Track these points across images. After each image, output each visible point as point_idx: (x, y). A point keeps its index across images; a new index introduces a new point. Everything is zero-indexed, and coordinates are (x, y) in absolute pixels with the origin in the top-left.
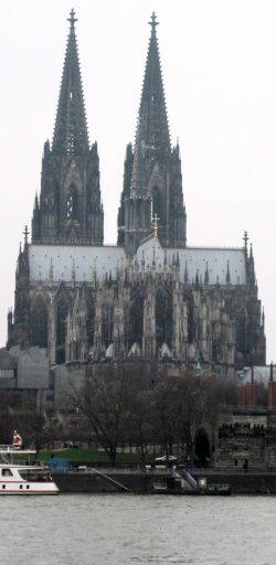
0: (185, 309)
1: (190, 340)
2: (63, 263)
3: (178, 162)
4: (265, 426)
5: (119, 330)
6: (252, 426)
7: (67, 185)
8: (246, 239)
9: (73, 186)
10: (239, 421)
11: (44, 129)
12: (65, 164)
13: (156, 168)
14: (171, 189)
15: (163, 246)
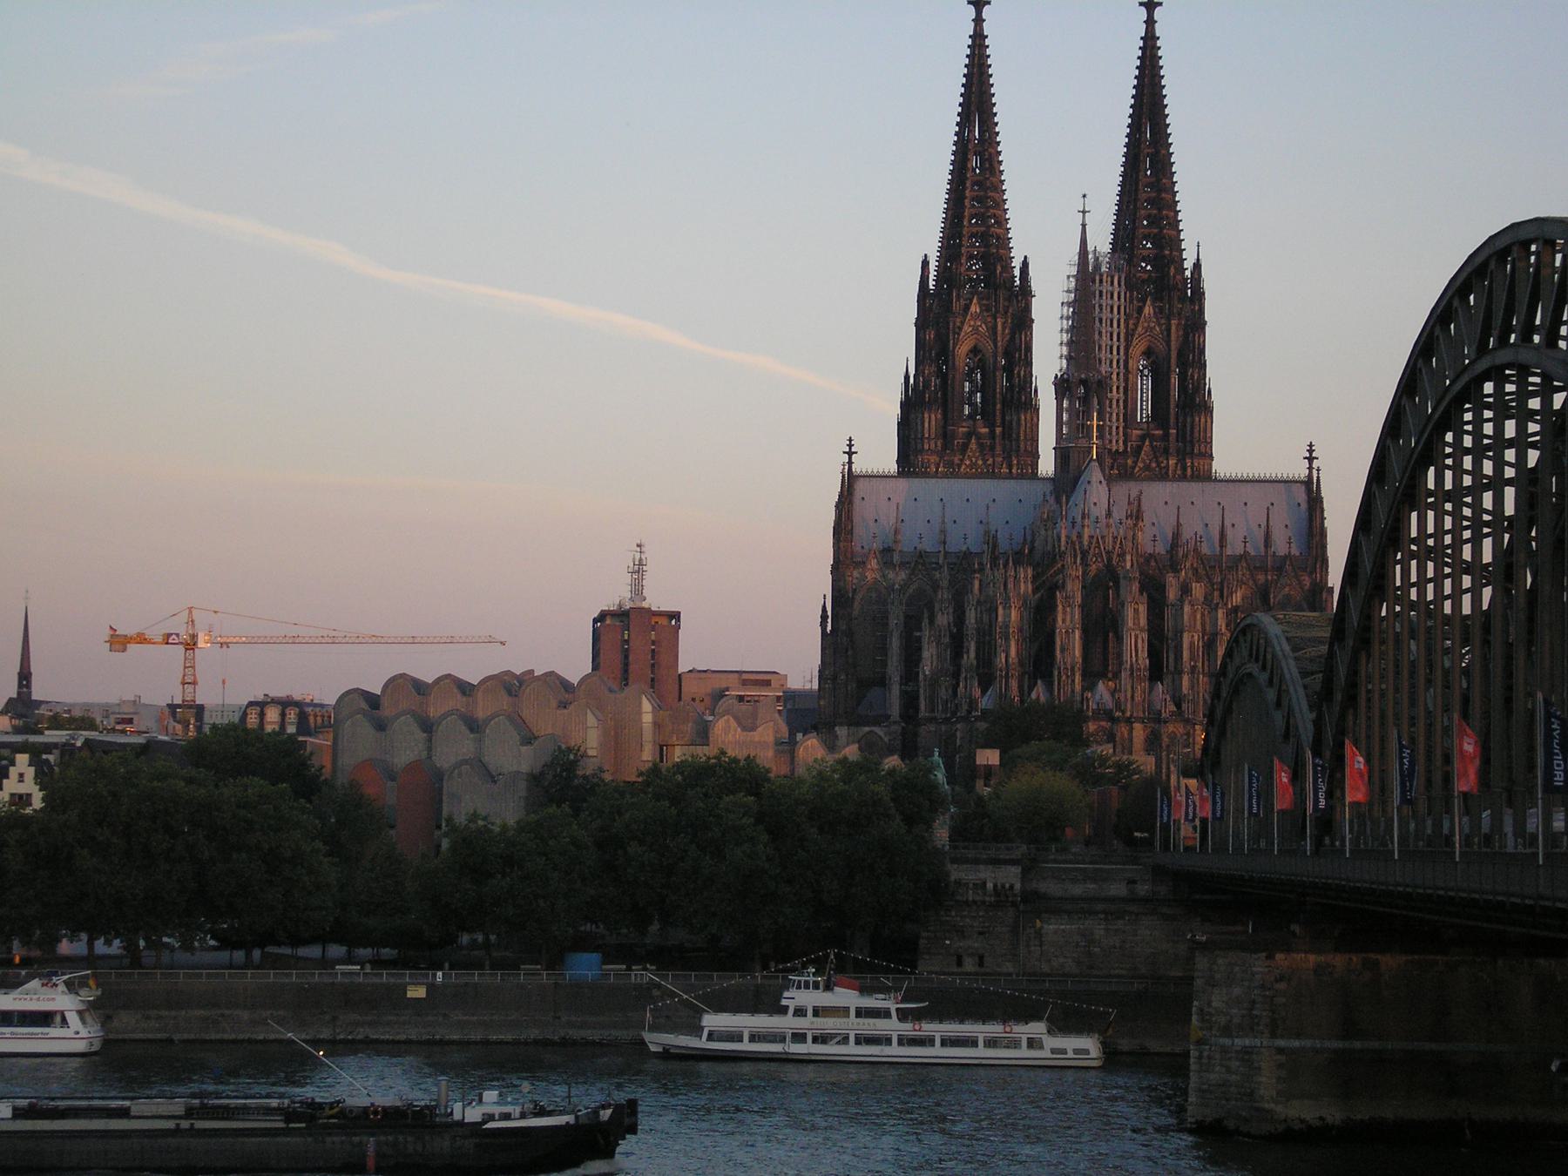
0: (1143, 609)
1: (1156, 672)
2: (969, 505)
3: (1199, 295)
4: (1018, 886)
5: (1010, 653)
6: (990, 885)
7: (962, 350)
8: (1311, 459)
9: (975, 351)
10: (963, 875)
11: (921, 232)
12: (957, 306)
13: (1148, 310)
14: (1180, 354)
15: (1110, 480)
